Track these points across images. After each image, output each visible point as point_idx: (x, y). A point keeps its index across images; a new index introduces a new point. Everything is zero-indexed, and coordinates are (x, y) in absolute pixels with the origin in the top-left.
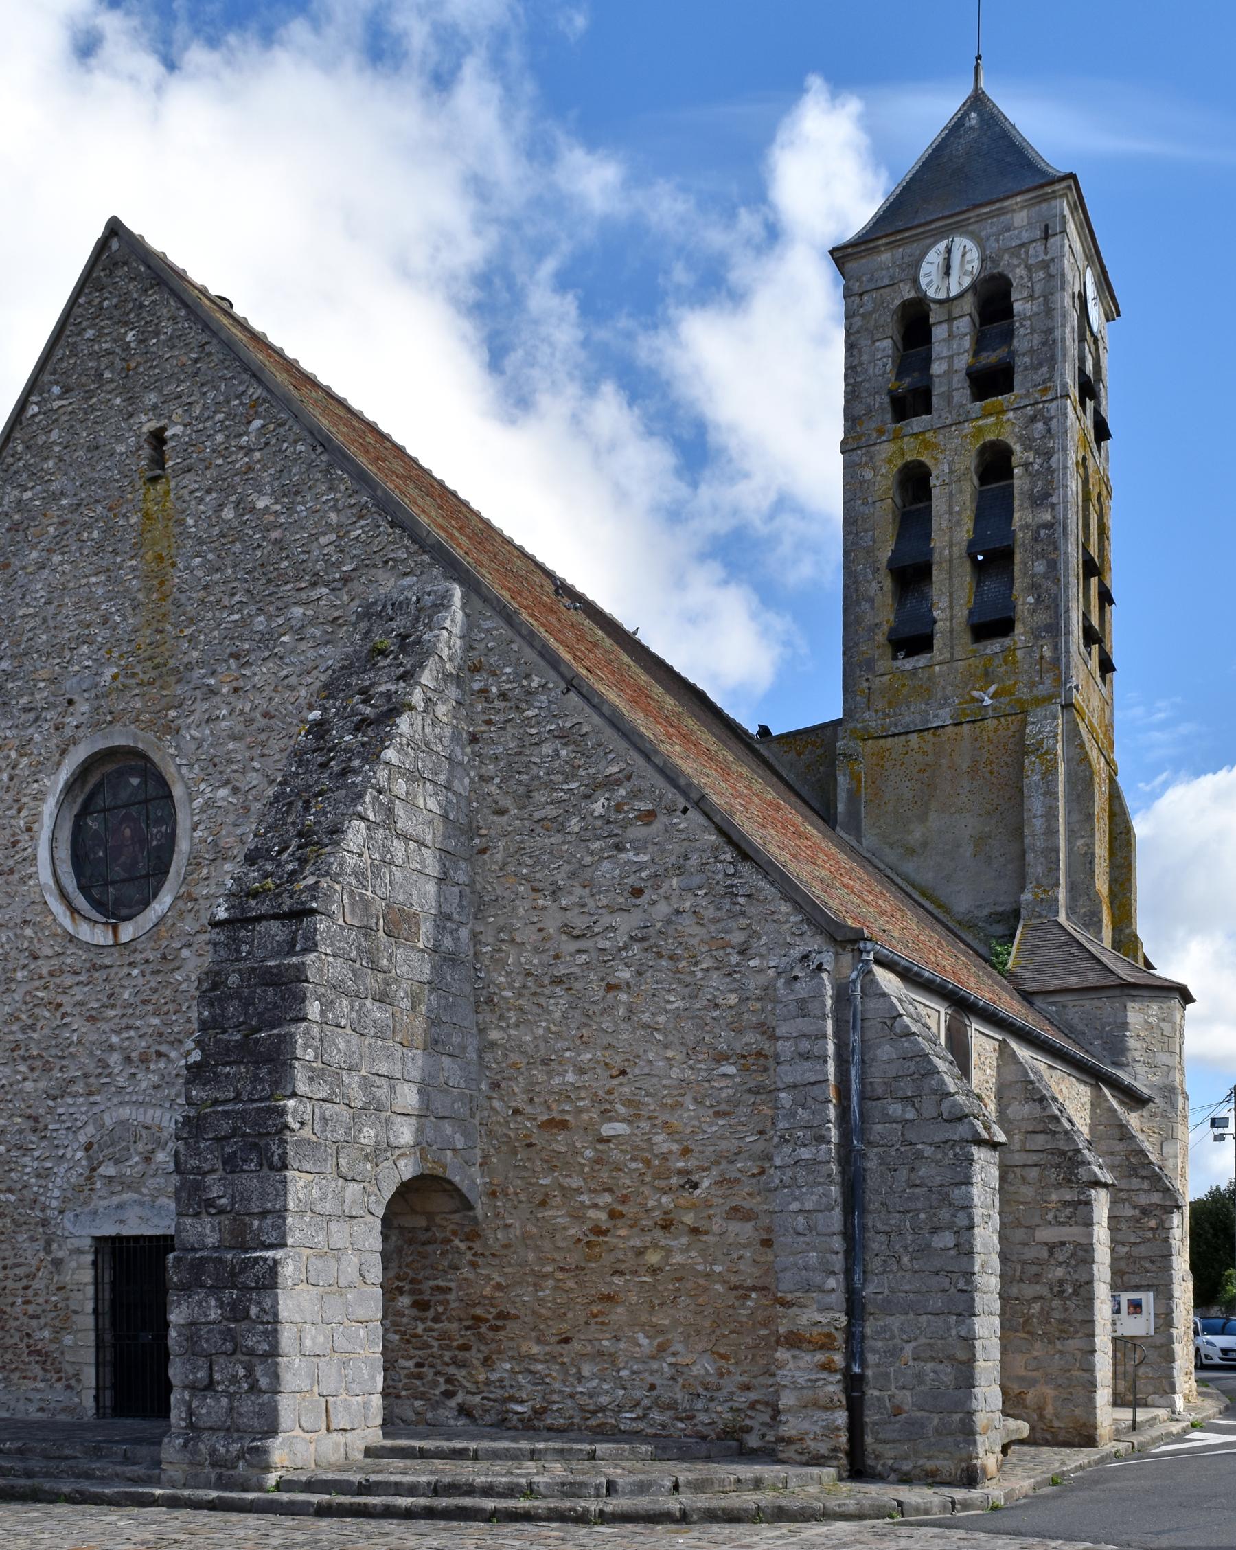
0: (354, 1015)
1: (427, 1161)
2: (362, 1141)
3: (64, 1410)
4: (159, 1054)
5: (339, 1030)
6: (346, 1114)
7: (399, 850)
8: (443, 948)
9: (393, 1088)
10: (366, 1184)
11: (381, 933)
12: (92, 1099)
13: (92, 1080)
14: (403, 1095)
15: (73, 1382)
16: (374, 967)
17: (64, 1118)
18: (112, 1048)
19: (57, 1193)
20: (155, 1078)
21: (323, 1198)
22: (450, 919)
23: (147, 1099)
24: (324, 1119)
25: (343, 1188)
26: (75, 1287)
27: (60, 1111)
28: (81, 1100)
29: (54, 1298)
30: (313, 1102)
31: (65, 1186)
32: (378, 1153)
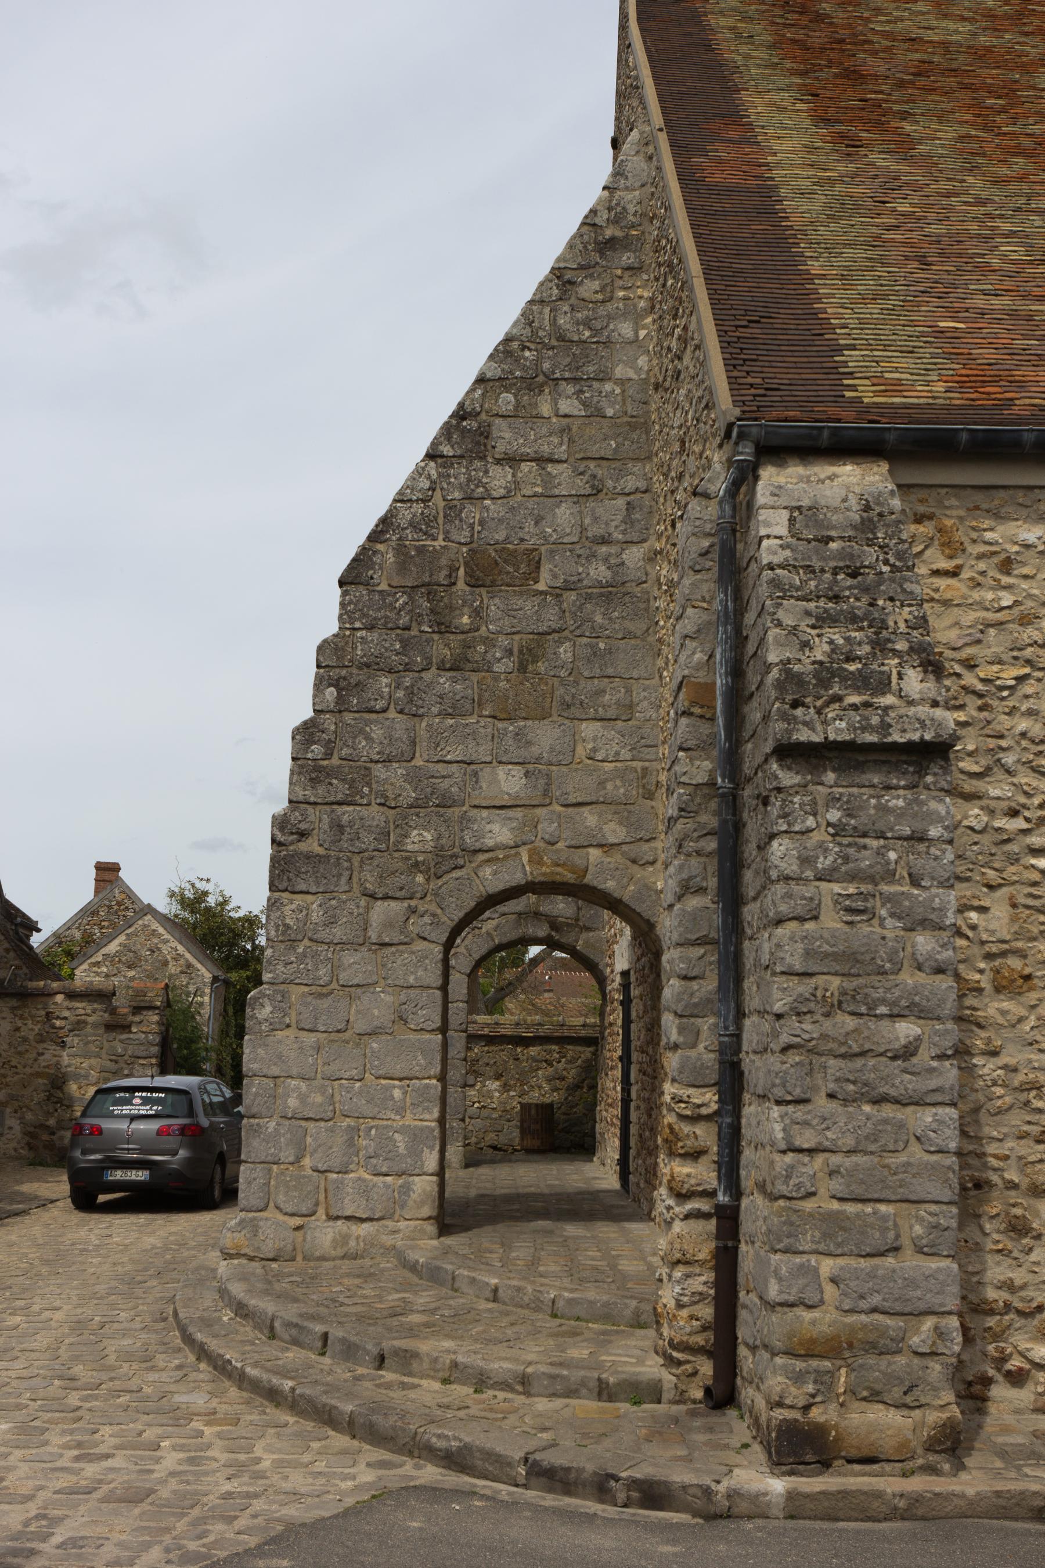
0: (400, 694)
1: (540, 863)
2: (409, 847)
5: (374, 716)
6: (375, 815)
7: (499, 478)
8: (585, 582)
9: (475, 774)
10: (413, 903)
11: (461, 585)
14: (495, 781)
16: (443, 627)
21: (331, 922)
22: (604, 541)
24: (339, 827)
25: (368, 909)
30: (319, 807)
32: (445, 860)
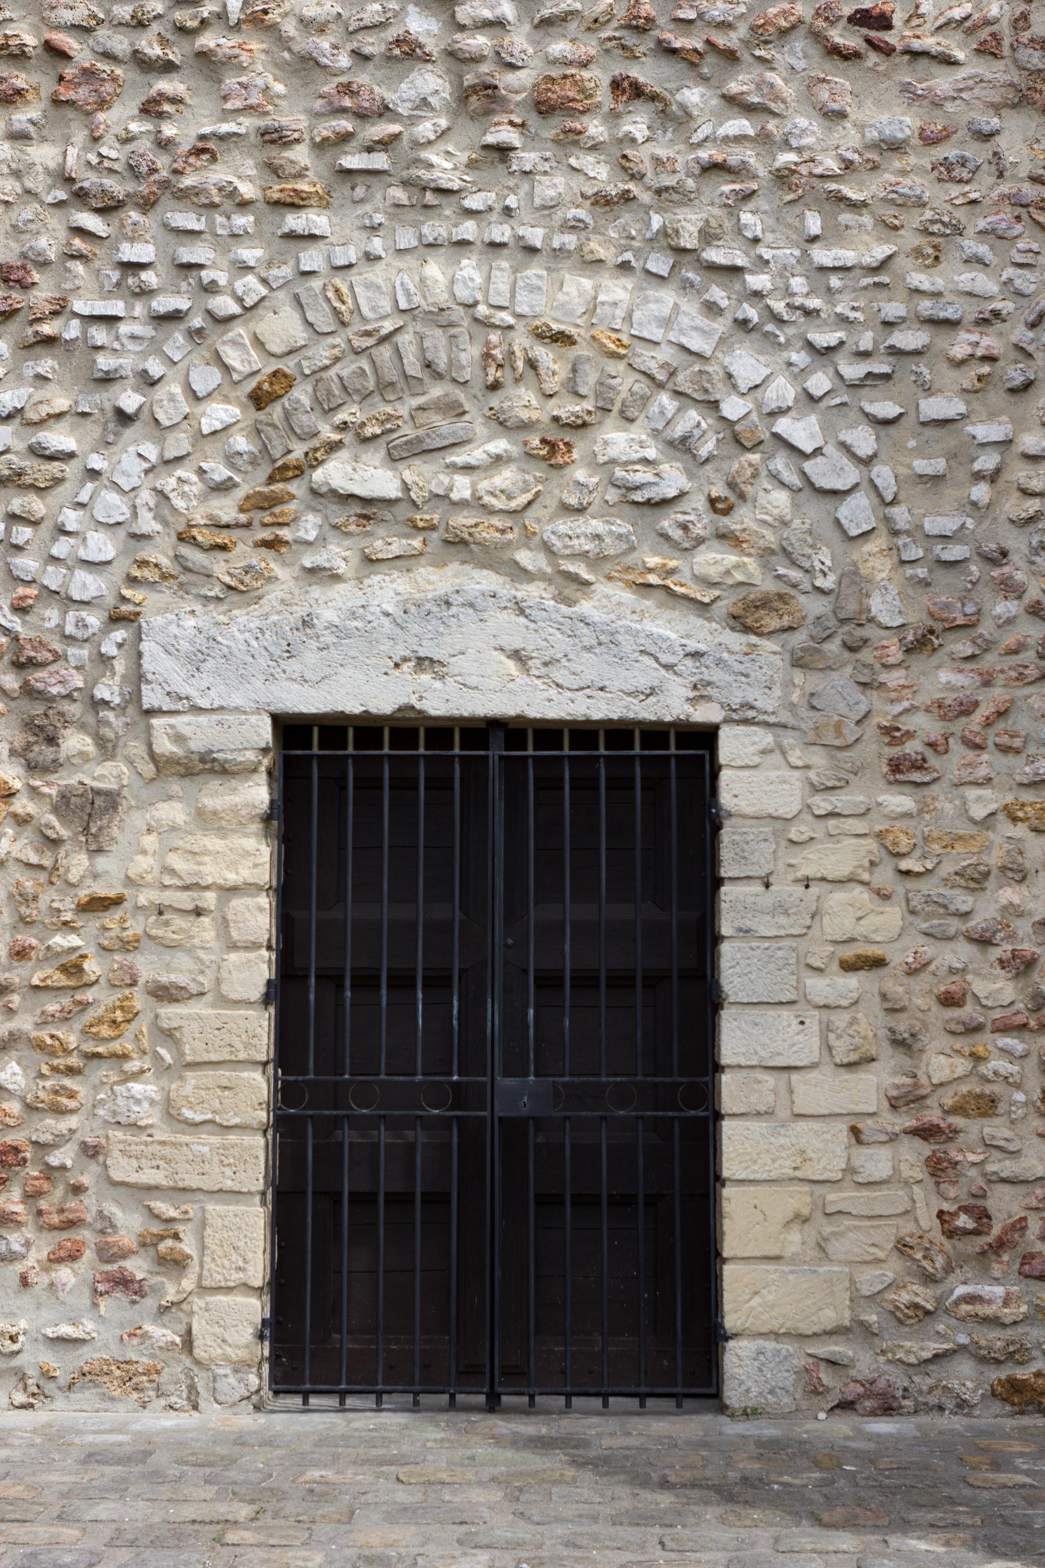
3: (87, 1377)
4: (629, 90)
12: (294, 222)
13: (301, 155)
15: (137, 1267)
17: (149, 277)
18: (408, 52)
19: (101, 546)
20: (600, 172)
23: (570, 240)
26: (185, 900)
27: (130, 252)
28: (243, 221)
29: (61, 941)
31: (147, 523)
